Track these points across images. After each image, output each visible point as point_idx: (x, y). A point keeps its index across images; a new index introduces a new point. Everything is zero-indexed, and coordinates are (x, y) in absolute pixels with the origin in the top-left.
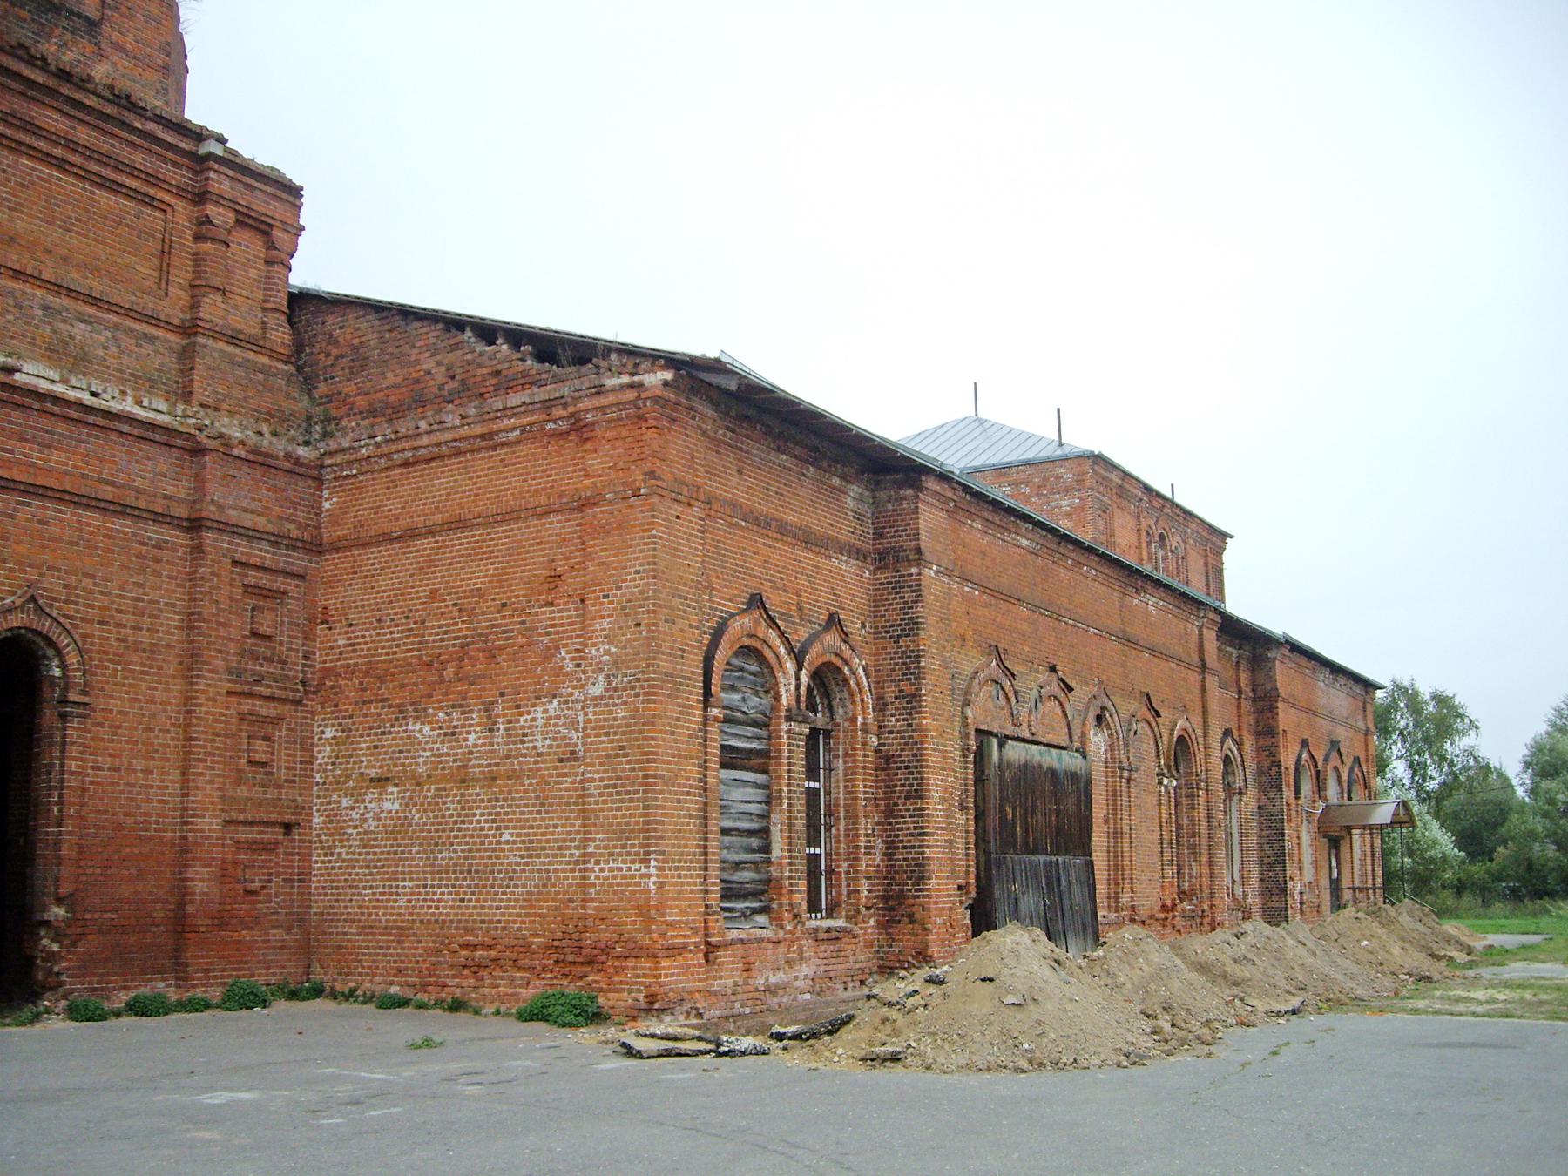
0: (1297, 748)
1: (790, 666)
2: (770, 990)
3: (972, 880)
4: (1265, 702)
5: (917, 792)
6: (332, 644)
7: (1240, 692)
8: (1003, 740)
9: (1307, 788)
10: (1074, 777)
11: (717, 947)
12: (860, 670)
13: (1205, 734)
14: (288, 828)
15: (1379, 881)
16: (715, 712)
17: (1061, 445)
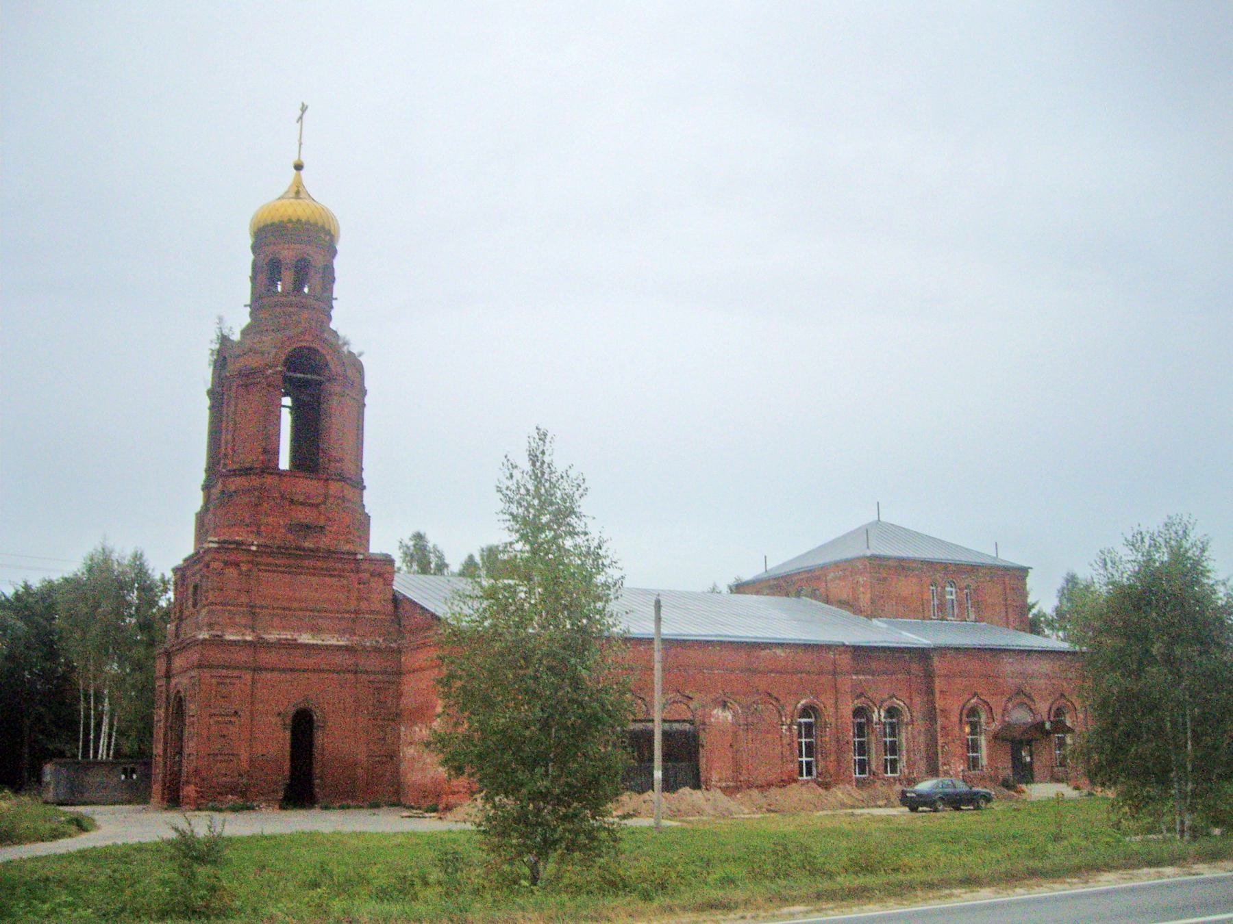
4: (929, 676)
6: (404, 701)
14: (391, 757)
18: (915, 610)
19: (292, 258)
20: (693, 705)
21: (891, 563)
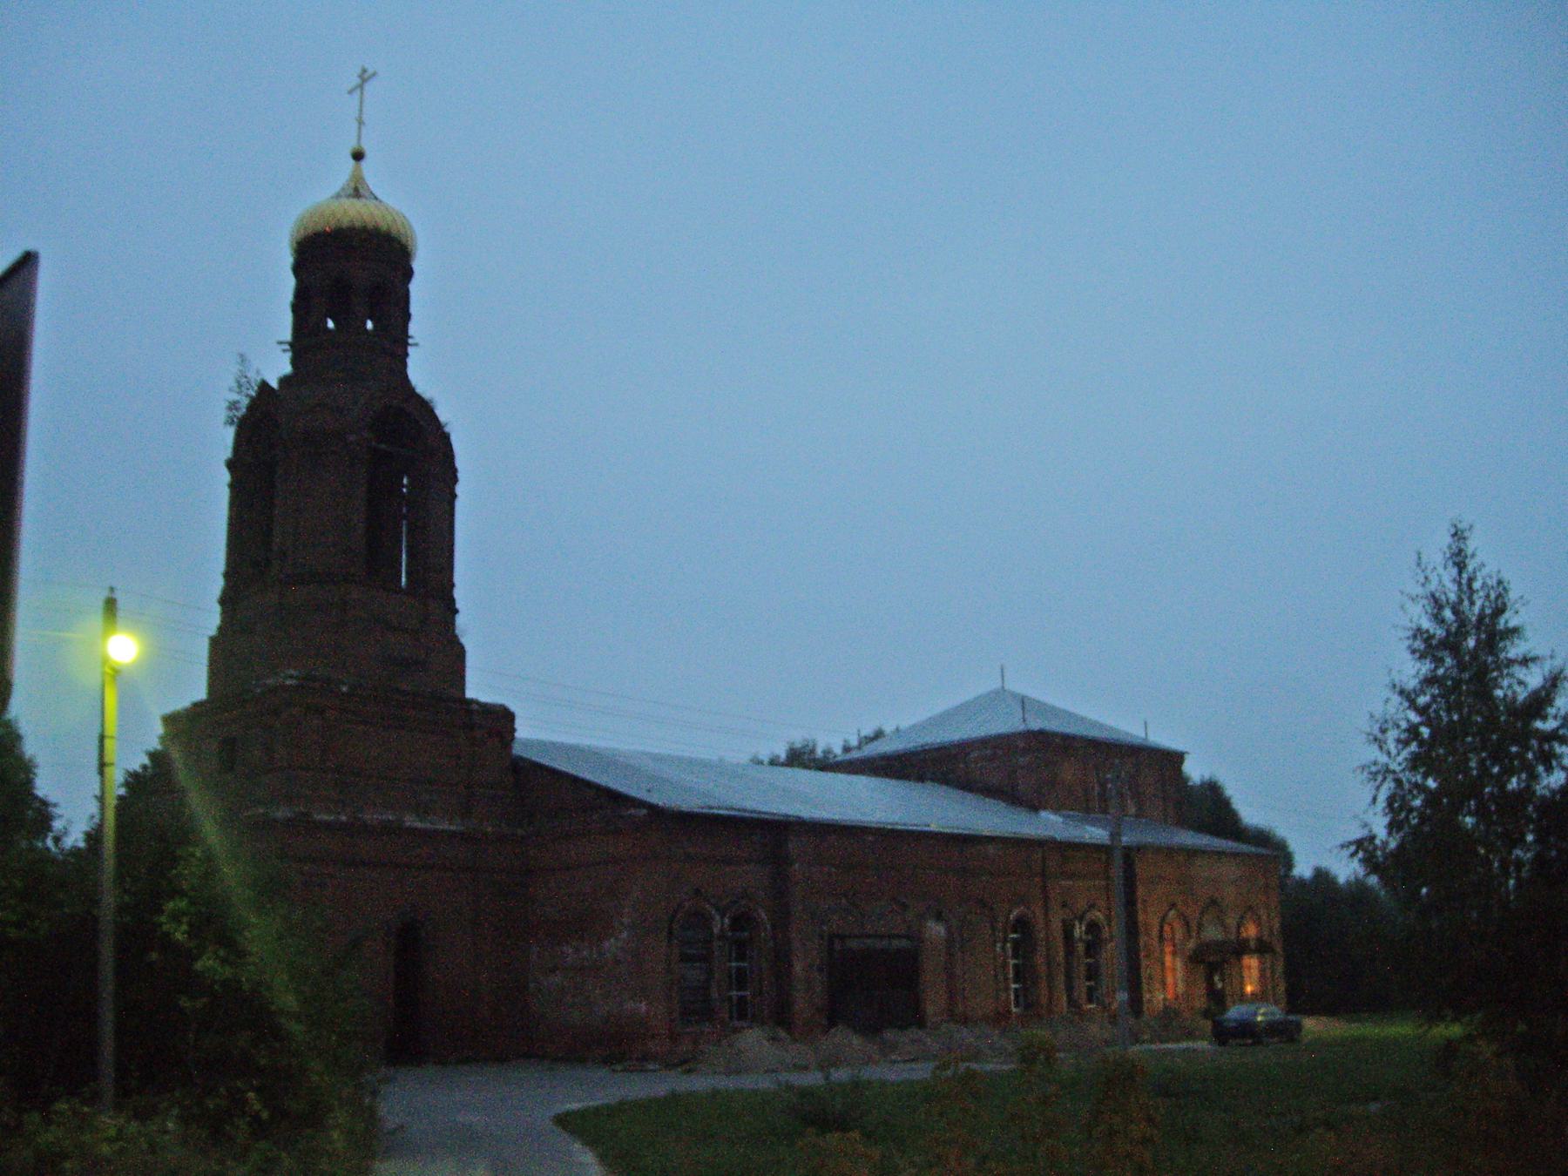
1: (718, 917)
8: (842, 938)
18: (1084, 804)
19: (353, 279)
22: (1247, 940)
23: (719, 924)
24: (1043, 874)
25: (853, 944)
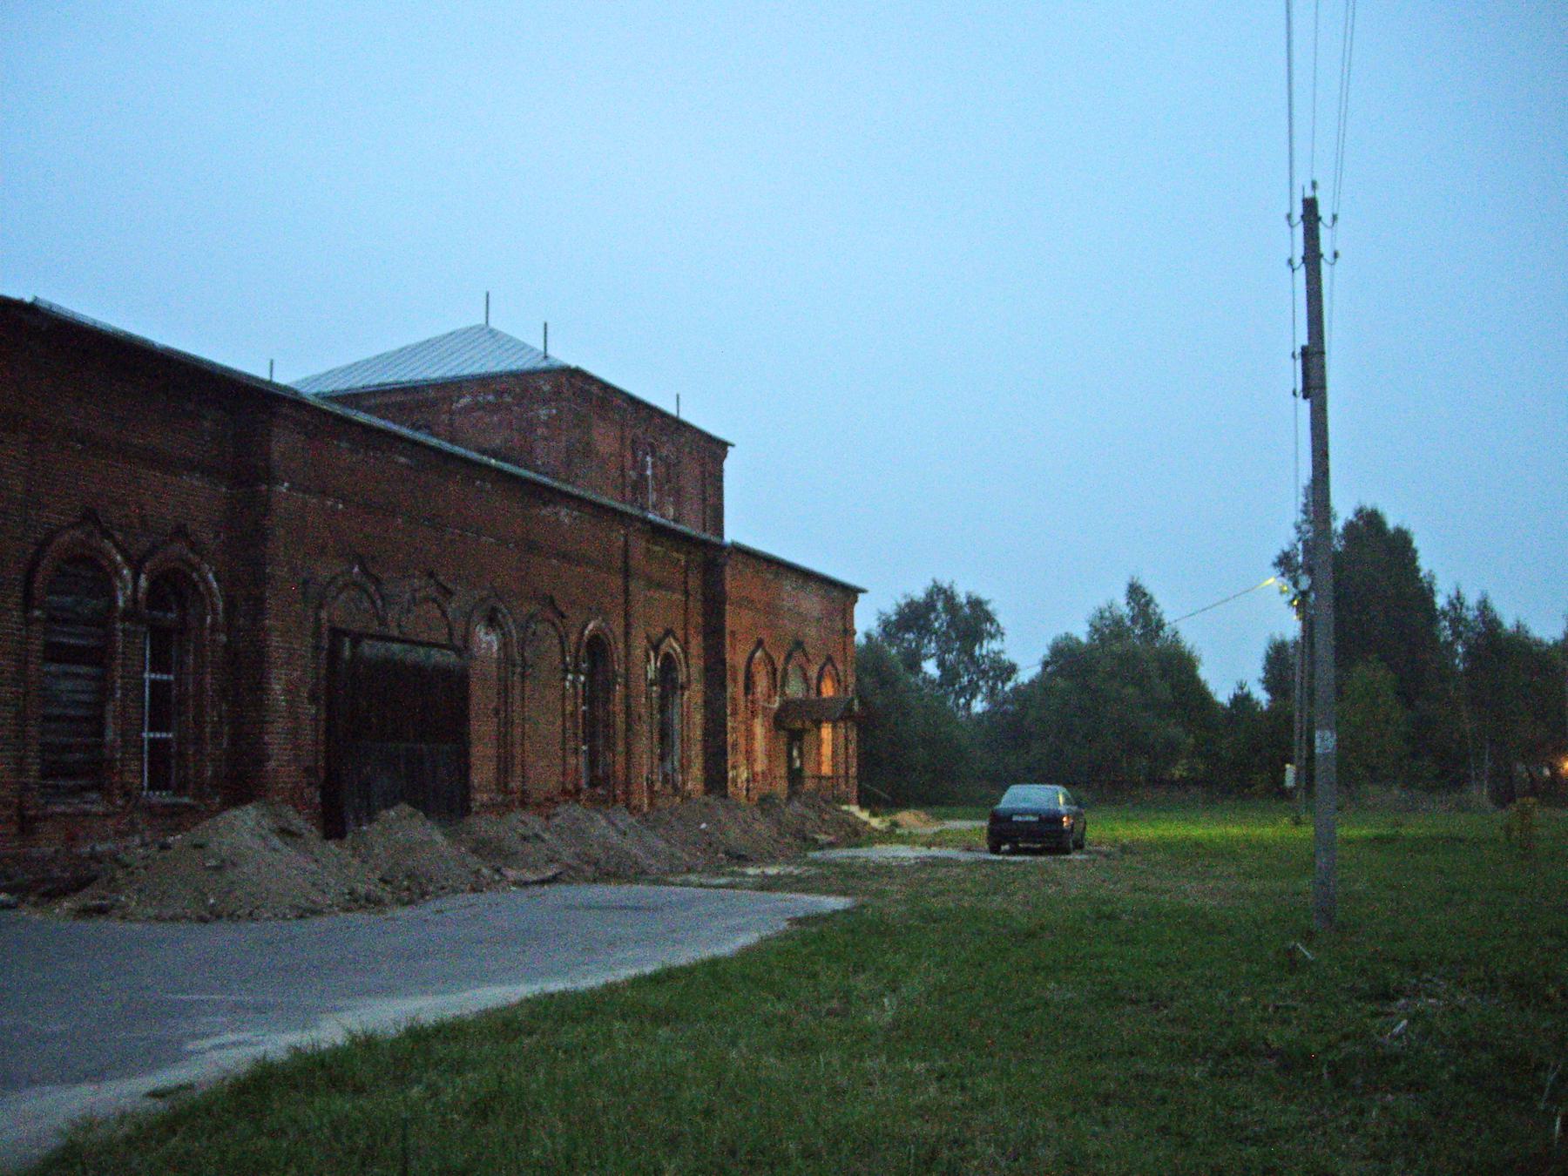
0: (750, 647)
2: (95, 857)
3: (321, 763)
4: (714, 605)
5: (260, 686)
7: (686, 593)
9: (762, 684)
10: (445, 673)
11: (36, 818)
12: (210, 575)
13: (627, 634)
15: (853, 771)
16: (37, 613)
17: (546, 357)
20: (452, 608)
21: (594, 388)
22: (821, 702)
23: (128, 587)
24: (627, 574)
25: (368, 648)
